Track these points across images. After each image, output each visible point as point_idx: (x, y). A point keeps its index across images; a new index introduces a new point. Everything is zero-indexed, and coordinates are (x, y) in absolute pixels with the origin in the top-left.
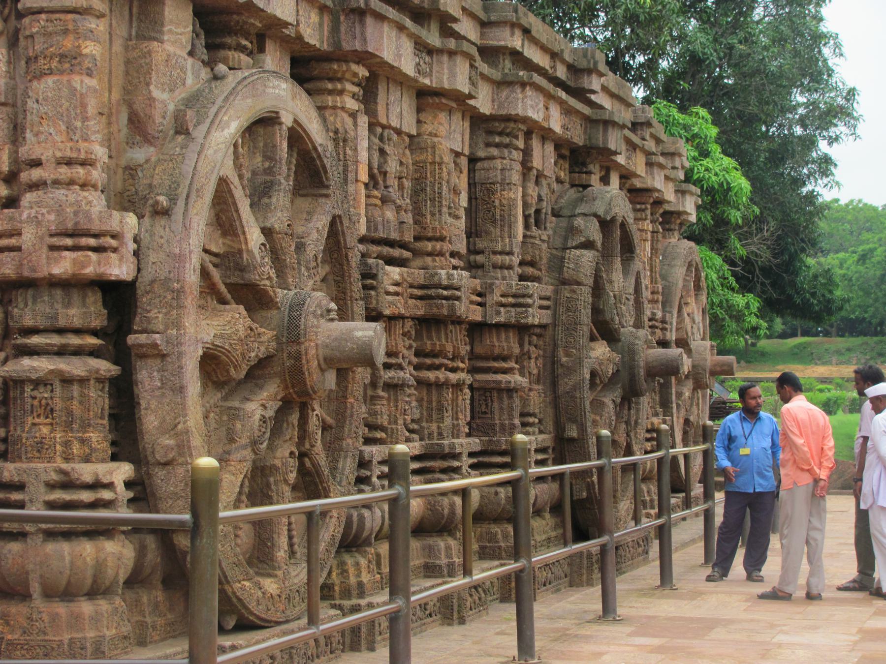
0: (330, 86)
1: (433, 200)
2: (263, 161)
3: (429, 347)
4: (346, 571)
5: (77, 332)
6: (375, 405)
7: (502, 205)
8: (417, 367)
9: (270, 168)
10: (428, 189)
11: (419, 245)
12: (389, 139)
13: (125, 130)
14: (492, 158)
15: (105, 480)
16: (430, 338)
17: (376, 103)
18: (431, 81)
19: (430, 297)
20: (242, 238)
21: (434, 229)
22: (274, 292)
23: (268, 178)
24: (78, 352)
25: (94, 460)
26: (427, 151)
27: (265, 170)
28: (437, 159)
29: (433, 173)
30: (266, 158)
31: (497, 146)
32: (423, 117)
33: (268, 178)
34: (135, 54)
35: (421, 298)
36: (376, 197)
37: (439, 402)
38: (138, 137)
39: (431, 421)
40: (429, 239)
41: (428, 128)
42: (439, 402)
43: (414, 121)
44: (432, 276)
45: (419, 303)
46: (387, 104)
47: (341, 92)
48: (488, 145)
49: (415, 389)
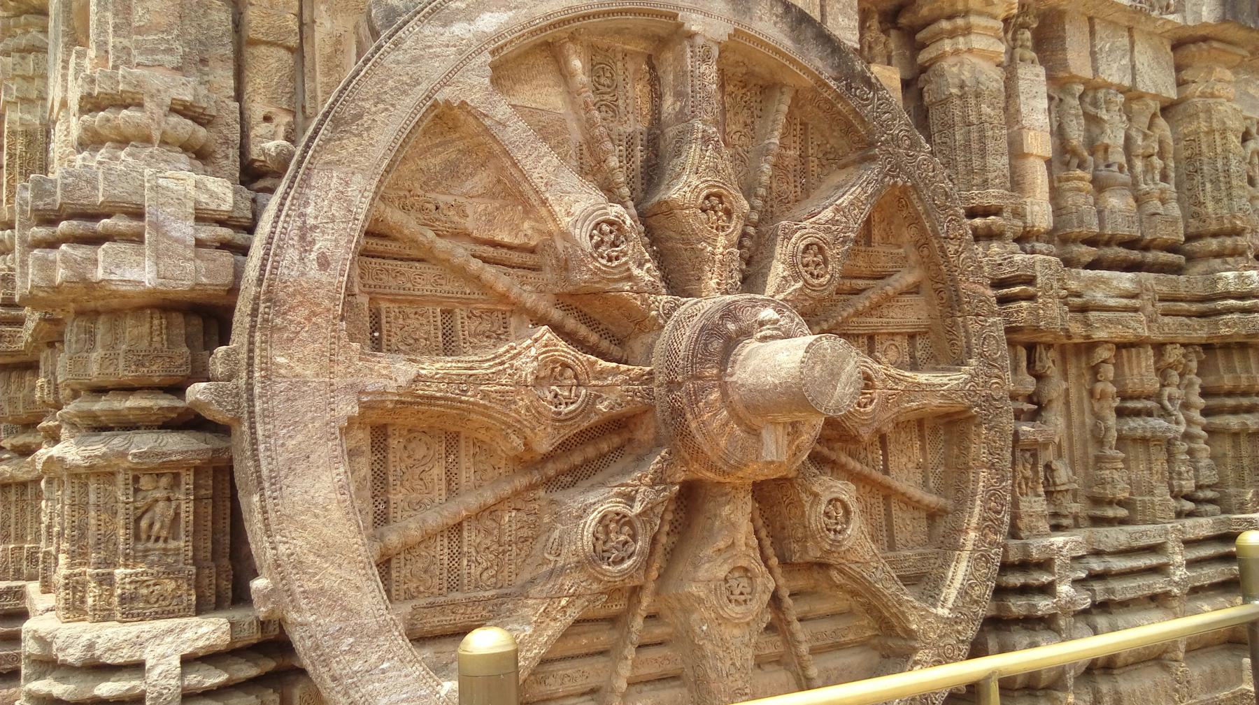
0: (945, 25)
3: (1227, 382)
5: (127, 389)
6: (1101, 469)
8: (1206, 412)
9: (682, 109)
10: (1205, 168)
11: (1197, 245)
12: (1108, 102)
15: (109, 659)
16: (1231, 369)
17: (1064, 50)
18: (1184, 18)
20: (544, 212)
21: (1220, 219)
22: (644, 300)
23: (680, 127)
24: (127, 425)
26: (1198, 118)
28: (1215, 125)
29: (1212, 146)
30: (679, 95)
32: (1187, 75)
35: (1202, 315)
36: (1081, 179)
39: (1243, 486)
40: (1215, 235)
41: (1195, 89)
43: (1171, 80)
44: (1215, 282)
45: (1195, 322)
46: (1093, 54)
47: (967, 31)
49: (1206, 443)
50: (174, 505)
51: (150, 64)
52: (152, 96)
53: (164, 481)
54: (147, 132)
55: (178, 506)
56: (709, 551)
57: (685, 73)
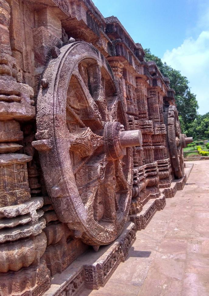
1: (142, 104)
2: (93, 79)
4: (133, 206)
7: (155, 108)
13: (34, 61)
14: (152, 97)
19: (145, 128)
23: (96, 85)
25: (19, 203)
27: (94, 82)
30: (94, 78)
31: (153, 95)
33: (96, 85)
34: (36, 33)
36: (129, 102)
37: (149, 154)
38: (39, 63)
42: (149, 154)
48: (151, 95)
50: (23, 172)
51: (7, 53)
52: (10, 62)
53: (22, 166)
54: (9, 72)
55: (25, 174)
56: (110, 175)
57: (97, 73)
